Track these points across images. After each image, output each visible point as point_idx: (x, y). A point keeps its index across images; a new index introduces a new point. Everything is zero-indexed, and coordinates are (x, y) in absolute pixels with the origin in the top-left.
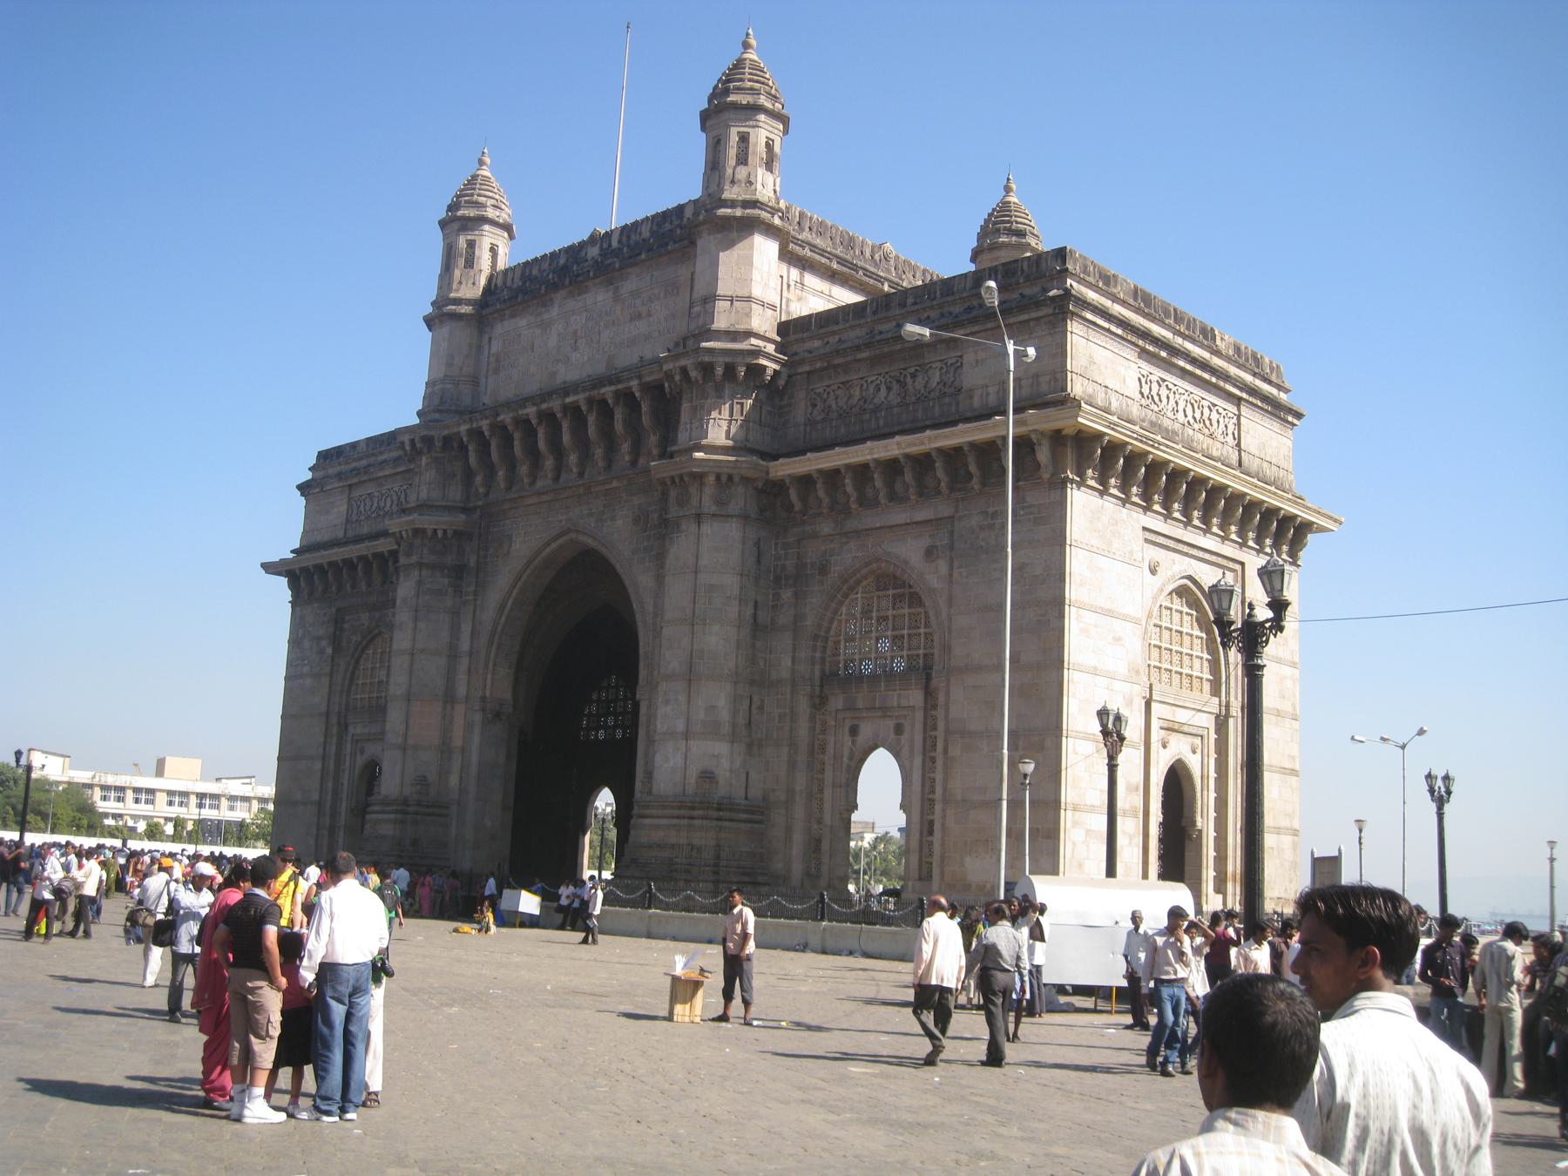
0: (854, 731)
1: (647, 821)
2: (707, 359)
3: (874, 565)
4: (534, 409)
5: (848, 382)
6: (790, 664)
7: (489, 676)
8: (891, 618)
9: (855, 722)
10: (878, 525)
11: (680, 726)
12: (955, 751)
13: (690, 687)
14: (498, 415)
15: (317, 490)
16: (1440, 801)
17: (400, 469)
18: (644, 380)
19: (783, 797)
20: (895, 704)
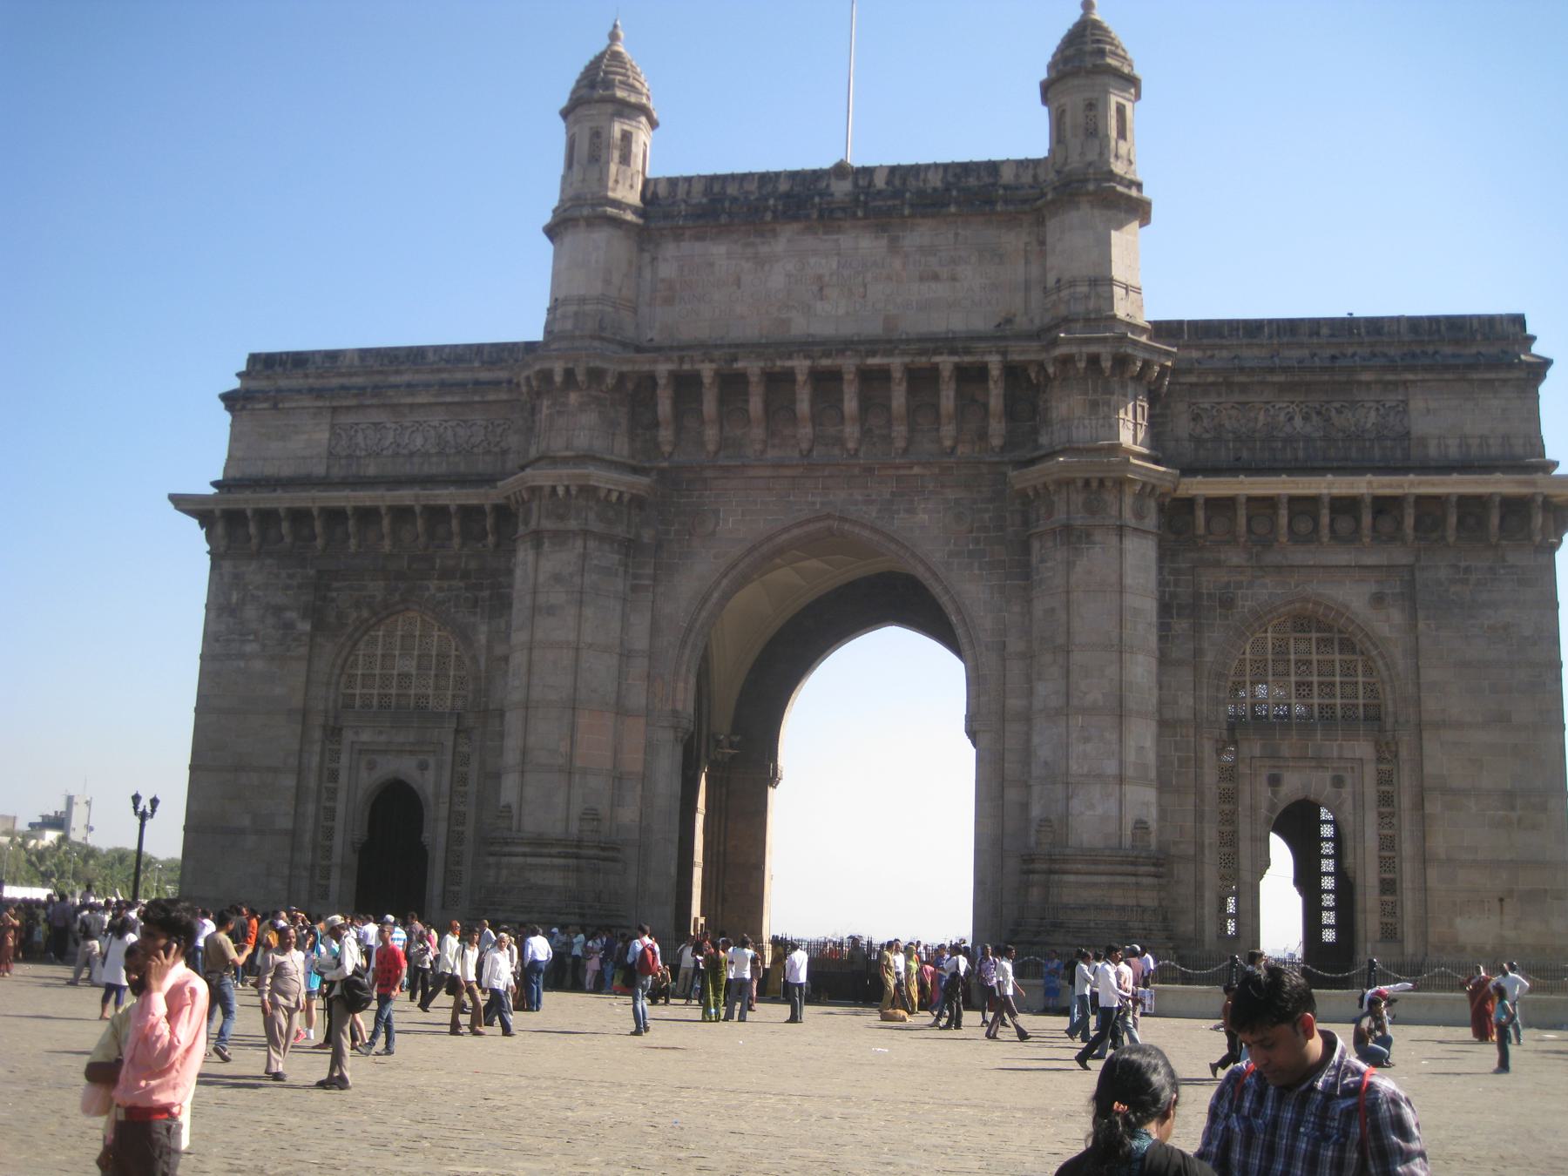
0: (1275, 781)
1: (1072, 878)
2: (1130, 351)
3: (1298, 605)
4: (808, 363)
5: (1248, 403)
6: (1191, 702)
7: (681, 685)
8: (1315, 664)
9: (1275, 771)
10: (1311, 563)
11: (1111, 768)
12: (1434, 807)
13: (1121, 724)
14: (735, 359)
15: (265, 405)
17: (449, 399)
18: (1009, 358)
19: (1191, 852)
20: (1335, 755)
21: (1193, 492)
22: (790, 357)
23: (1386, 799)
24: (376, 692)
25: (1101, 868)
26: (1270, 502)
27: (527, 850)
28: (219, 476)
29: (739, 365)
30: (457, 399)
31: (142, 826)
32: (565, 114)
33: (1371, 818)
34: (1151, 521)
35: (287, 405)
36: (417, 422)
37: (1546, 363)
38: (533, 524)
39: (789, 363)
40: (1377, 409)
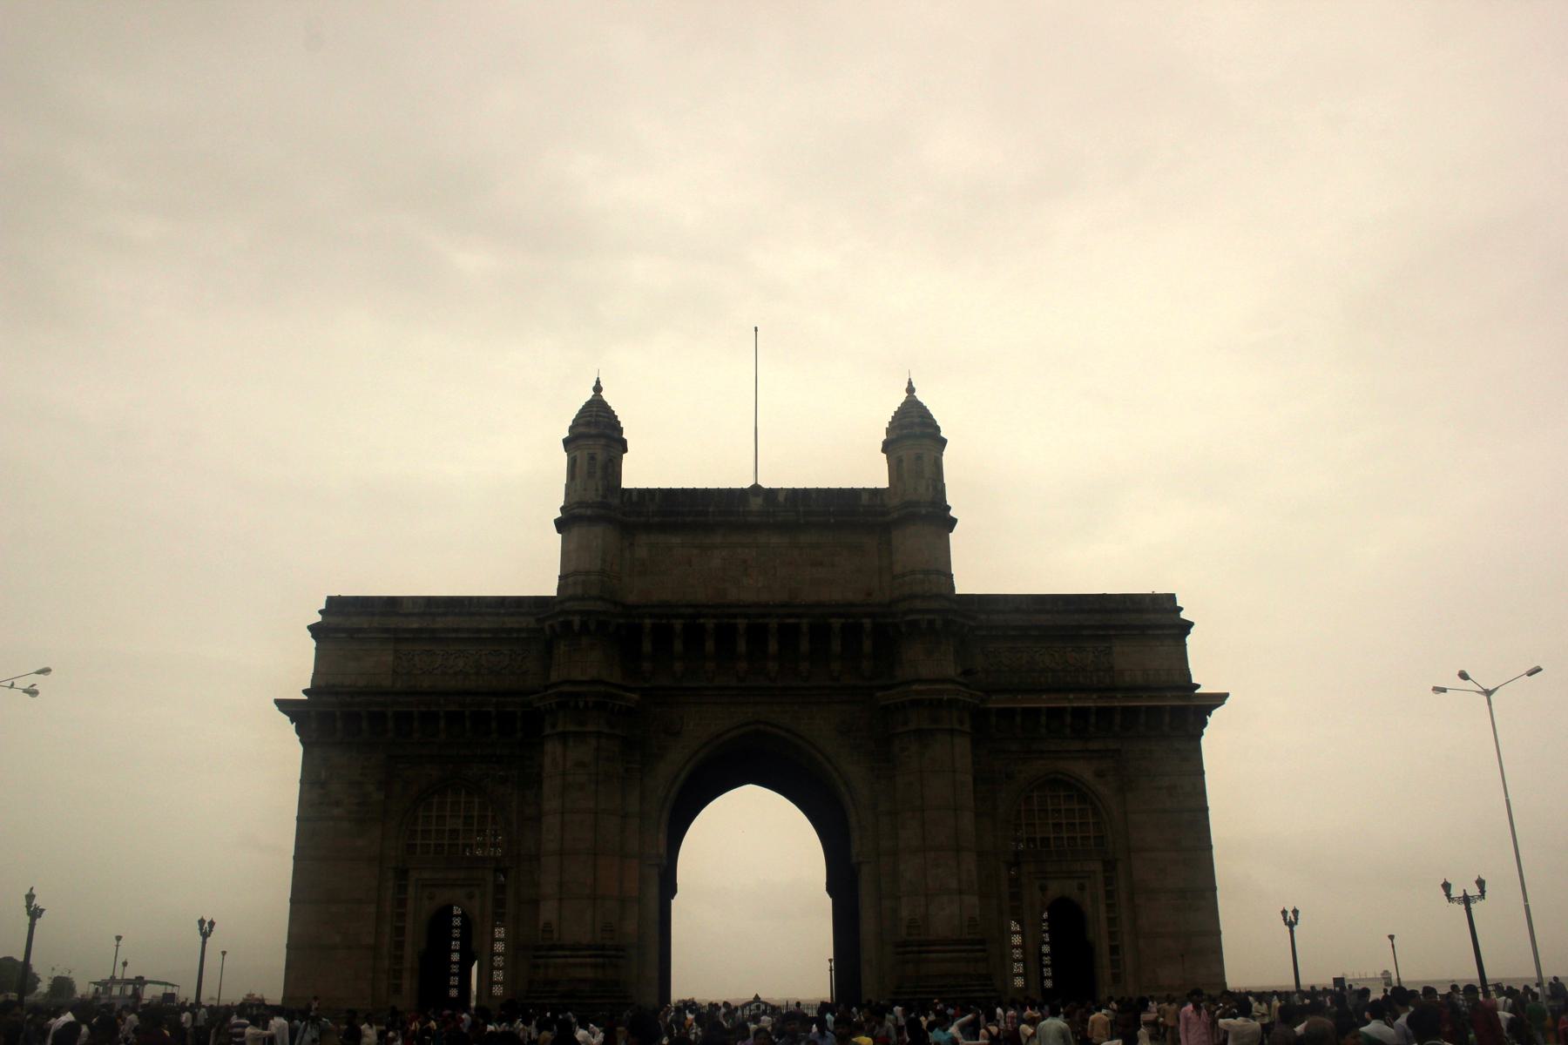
0: (1043, 889)
16: (1291, 925)
21: (990, 706)
22: (735, 616)
23: (1109, 895)
24: (432, 842)
25: (951, 948)
26: (1037, 711)
27: (568, 953)
28: (308, 686)
29: (702, 621)
30: (489, 635)
31: (204, 943)
32: (566, 442)
33: (1102, 908)
34: (967, 727)
35: (360, 636)
36: (459, 650)
37: (1191, 624)
38: (560, 729)
39: (733, 621)
40: (1094, 653)
